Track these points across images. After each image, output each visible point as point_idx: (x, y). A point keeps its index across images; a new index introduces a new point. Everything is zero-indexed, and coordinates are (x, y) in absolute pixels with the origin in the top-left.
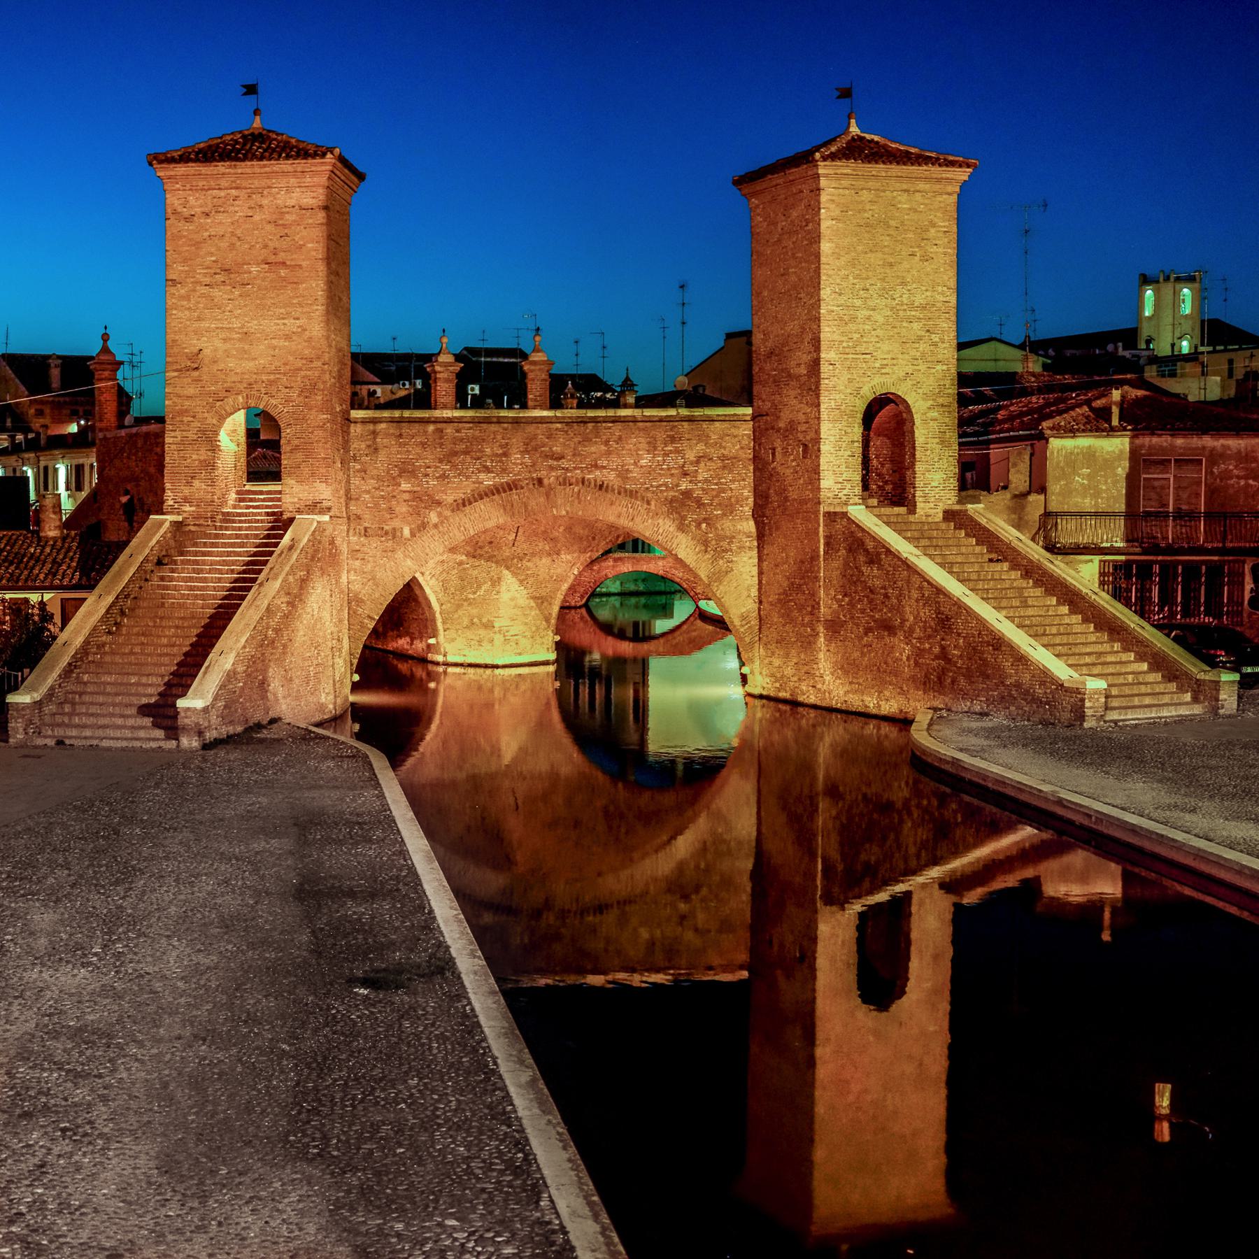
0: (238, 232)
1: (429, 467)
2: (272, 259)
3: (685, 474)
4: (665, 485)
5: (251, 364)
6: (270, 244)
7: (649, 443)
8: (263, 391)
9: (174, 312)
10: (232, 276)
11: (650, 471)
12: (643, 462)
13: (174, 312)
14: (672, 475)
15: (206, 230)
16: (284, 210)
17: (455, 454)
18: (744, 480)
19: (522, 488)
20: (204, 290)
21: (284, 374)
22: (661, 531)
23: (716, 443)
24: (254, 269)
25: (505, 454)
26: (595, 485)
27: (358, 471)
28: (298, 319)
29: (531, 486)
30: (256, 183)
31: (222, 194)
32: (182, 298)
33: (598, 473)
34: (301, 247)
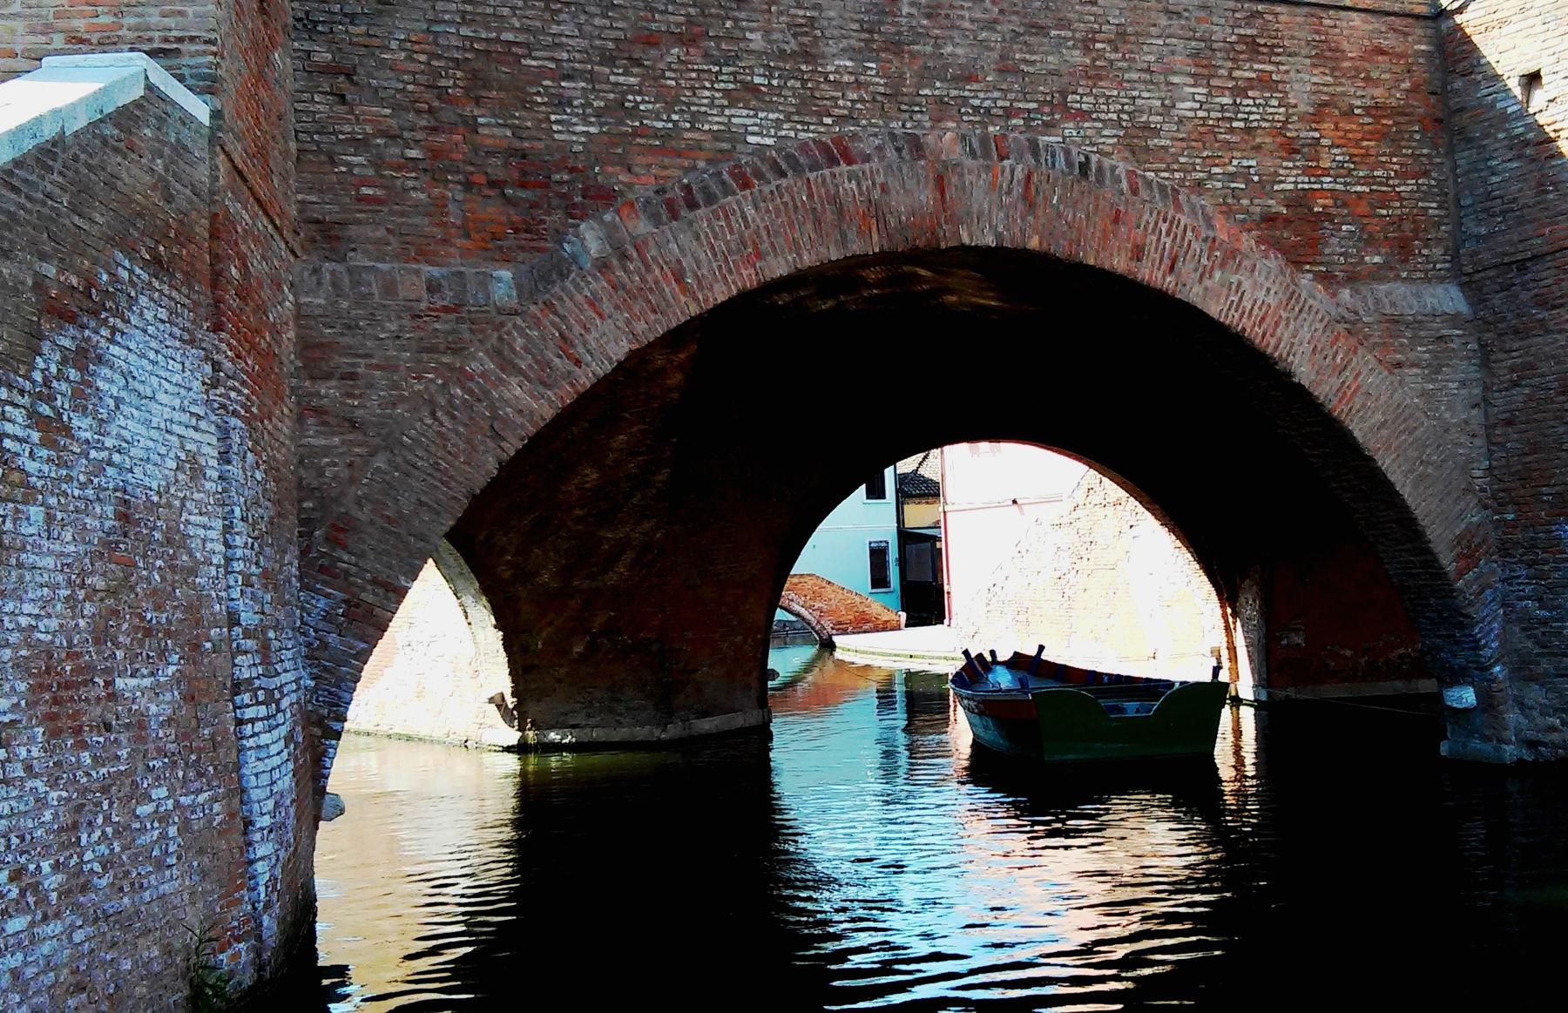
1: (569, 77)
3: (1291, 149)
4: (1244, 174)
7: (1195, 55)
11: (1203, 134)
12: (1184, 107)
14: (1258, 148)
17: (651, 41)
18: (1426, 174)
19: (867, 159)
22: (1247, 304)
23: (1356, 69)
25: (807, 55)
26: (1069, 164)
29: (890, 153)
33: (1069, 128)
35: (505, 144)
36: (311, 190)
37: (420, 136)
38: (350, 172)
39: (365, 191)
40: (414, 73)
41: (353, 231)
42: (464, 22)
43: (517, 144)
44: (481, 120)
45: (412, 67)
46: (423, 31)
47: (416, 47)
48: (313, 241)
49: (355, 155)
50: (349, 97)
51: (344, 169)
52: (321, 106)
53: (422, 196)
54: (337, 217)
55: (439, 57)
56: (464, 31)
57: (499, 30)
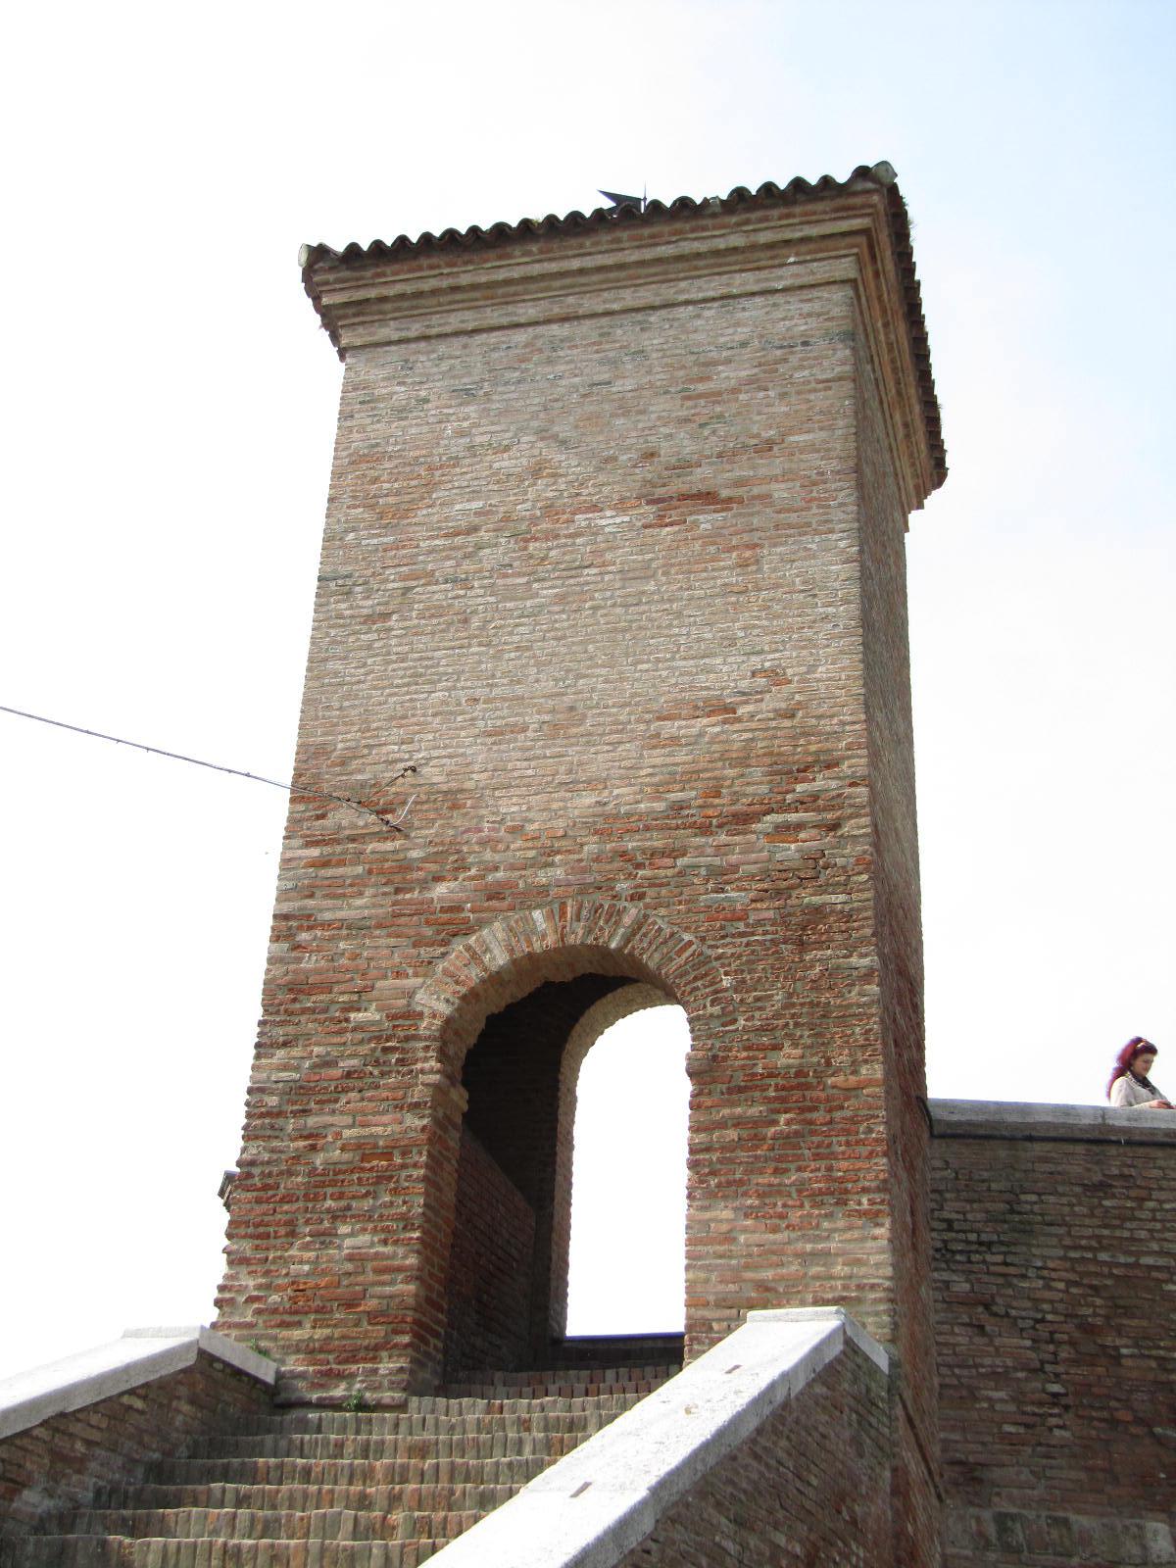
0: (562, 429)
2: (678, 486)
5: (588, 799)
6: (665, 449)
8: (623, 886)
9: (338, 665)
10: (532, 546)
13: (338, 665)
15: (461, 433)
16: (714, 355)
20: (440, 593)
21: (705, 830)
24: (609, 521)
27: (966, 1302)
28: (761, 652)
30: (629, 298)
31: (520, 337)
32: (369, 619)
34: (768, 446)
35: (1151, 1376)
36: (953, 1429)
37: (1060, 1369)
38: (992, 1407)
39: (1009, 1428)
40: (1052, 1302)
41: (996, 1474)
42: (1102, 1248)
43: (1163, 1377)
44: (1124, 1351)
45: (1047, 1295)
46: (1060, 1259)
47: (1054, 1275)
48: (956, 1484)
49: (996, 1389)
50: (988, 1328)
51: (985, 1405)
52: (962, 1338)
53: (1066, 1434)
54: (982, 1458)
55: (1076, 1284)
56: (1103, 1256)
57: (1138, 1254)
